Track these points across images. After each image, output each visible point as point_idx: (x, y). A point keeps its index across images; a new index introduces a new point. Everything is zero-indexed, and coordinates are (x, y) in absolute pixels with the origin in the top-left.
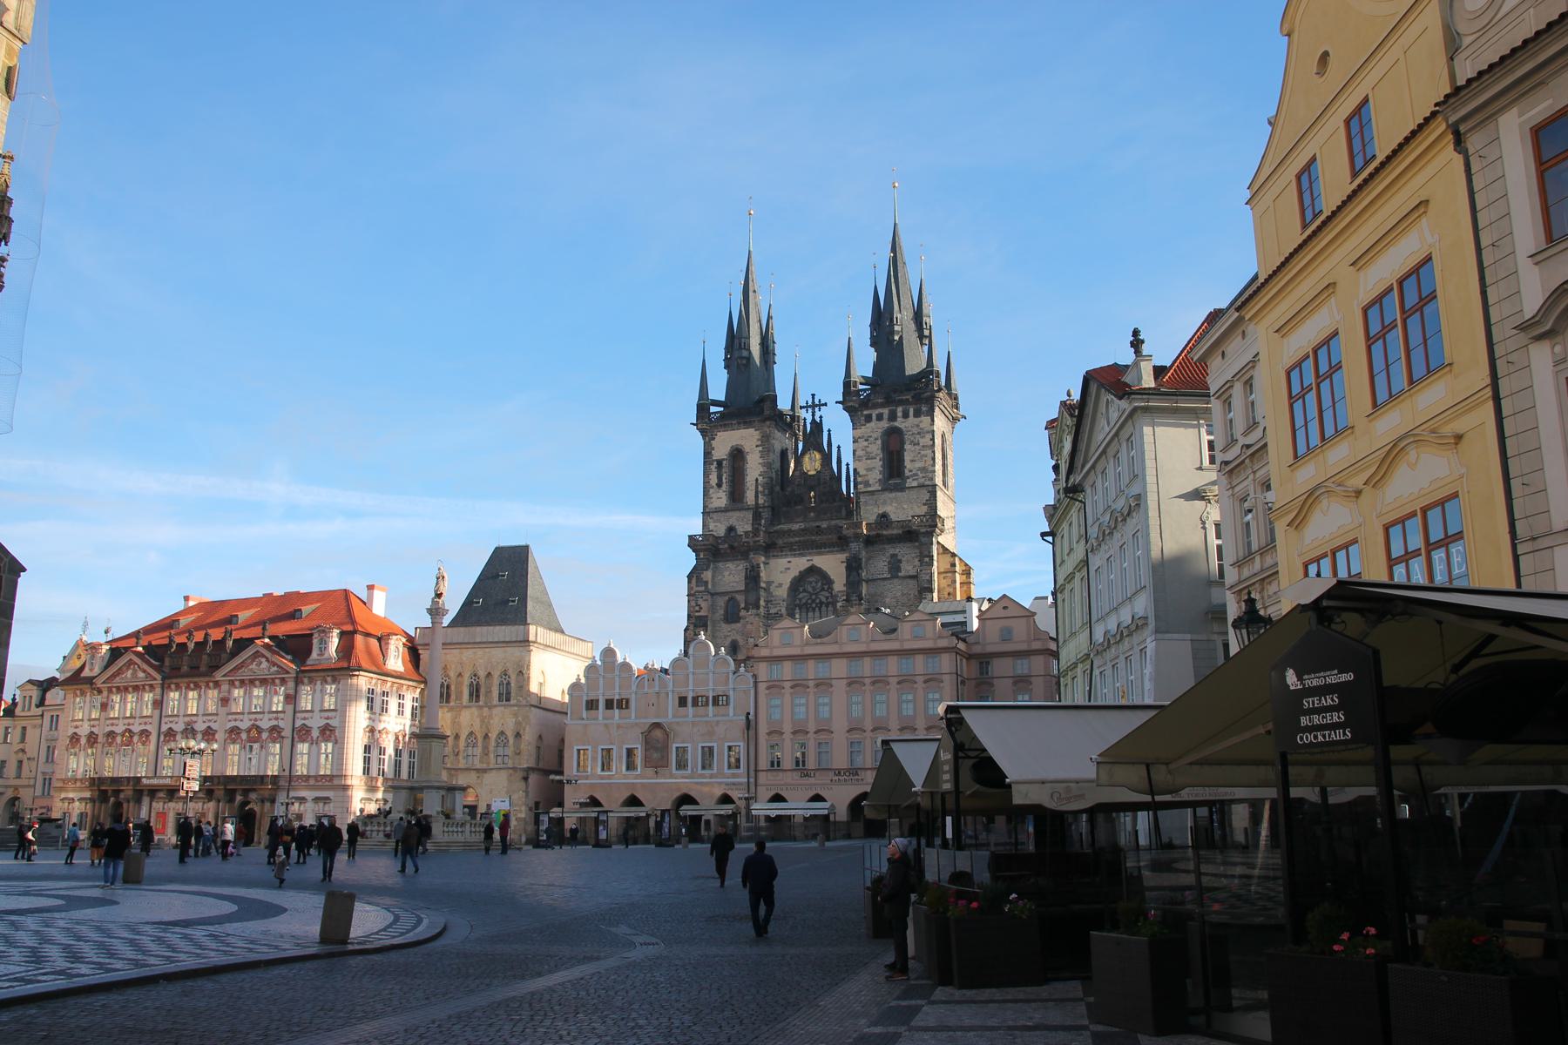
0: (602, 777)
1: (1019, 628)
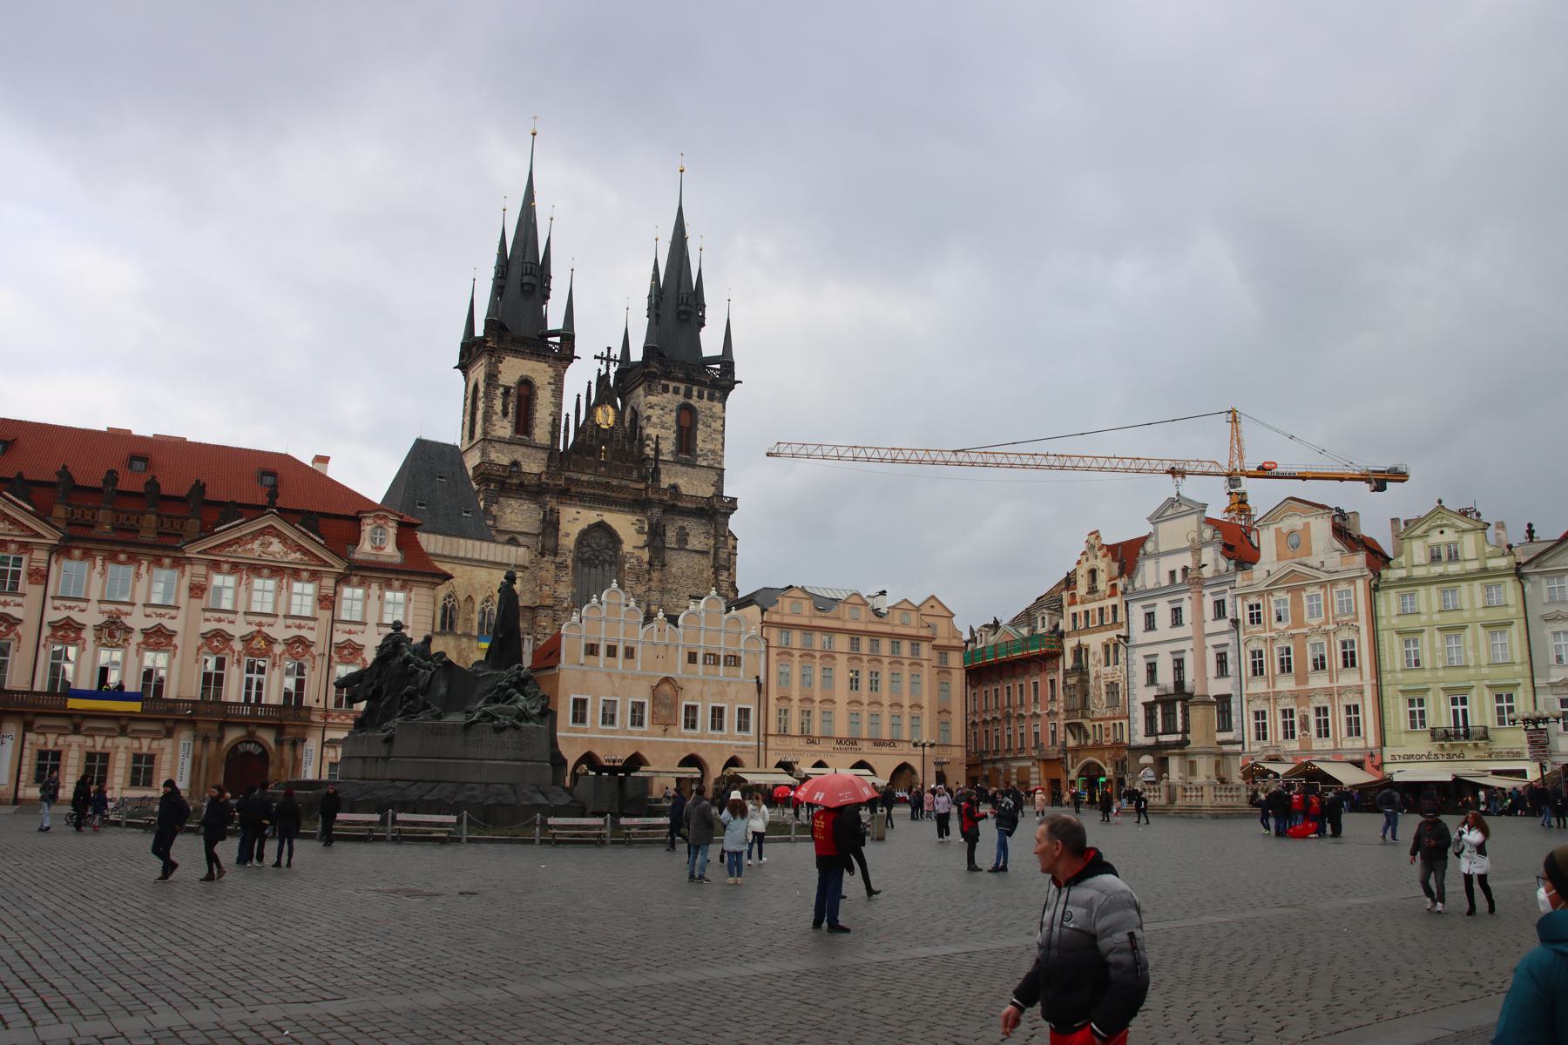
0: (630, 733)
1: (942, 625)
